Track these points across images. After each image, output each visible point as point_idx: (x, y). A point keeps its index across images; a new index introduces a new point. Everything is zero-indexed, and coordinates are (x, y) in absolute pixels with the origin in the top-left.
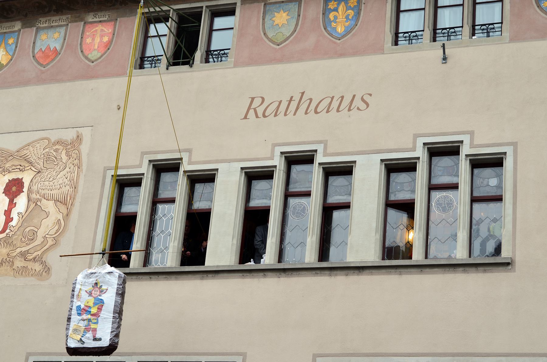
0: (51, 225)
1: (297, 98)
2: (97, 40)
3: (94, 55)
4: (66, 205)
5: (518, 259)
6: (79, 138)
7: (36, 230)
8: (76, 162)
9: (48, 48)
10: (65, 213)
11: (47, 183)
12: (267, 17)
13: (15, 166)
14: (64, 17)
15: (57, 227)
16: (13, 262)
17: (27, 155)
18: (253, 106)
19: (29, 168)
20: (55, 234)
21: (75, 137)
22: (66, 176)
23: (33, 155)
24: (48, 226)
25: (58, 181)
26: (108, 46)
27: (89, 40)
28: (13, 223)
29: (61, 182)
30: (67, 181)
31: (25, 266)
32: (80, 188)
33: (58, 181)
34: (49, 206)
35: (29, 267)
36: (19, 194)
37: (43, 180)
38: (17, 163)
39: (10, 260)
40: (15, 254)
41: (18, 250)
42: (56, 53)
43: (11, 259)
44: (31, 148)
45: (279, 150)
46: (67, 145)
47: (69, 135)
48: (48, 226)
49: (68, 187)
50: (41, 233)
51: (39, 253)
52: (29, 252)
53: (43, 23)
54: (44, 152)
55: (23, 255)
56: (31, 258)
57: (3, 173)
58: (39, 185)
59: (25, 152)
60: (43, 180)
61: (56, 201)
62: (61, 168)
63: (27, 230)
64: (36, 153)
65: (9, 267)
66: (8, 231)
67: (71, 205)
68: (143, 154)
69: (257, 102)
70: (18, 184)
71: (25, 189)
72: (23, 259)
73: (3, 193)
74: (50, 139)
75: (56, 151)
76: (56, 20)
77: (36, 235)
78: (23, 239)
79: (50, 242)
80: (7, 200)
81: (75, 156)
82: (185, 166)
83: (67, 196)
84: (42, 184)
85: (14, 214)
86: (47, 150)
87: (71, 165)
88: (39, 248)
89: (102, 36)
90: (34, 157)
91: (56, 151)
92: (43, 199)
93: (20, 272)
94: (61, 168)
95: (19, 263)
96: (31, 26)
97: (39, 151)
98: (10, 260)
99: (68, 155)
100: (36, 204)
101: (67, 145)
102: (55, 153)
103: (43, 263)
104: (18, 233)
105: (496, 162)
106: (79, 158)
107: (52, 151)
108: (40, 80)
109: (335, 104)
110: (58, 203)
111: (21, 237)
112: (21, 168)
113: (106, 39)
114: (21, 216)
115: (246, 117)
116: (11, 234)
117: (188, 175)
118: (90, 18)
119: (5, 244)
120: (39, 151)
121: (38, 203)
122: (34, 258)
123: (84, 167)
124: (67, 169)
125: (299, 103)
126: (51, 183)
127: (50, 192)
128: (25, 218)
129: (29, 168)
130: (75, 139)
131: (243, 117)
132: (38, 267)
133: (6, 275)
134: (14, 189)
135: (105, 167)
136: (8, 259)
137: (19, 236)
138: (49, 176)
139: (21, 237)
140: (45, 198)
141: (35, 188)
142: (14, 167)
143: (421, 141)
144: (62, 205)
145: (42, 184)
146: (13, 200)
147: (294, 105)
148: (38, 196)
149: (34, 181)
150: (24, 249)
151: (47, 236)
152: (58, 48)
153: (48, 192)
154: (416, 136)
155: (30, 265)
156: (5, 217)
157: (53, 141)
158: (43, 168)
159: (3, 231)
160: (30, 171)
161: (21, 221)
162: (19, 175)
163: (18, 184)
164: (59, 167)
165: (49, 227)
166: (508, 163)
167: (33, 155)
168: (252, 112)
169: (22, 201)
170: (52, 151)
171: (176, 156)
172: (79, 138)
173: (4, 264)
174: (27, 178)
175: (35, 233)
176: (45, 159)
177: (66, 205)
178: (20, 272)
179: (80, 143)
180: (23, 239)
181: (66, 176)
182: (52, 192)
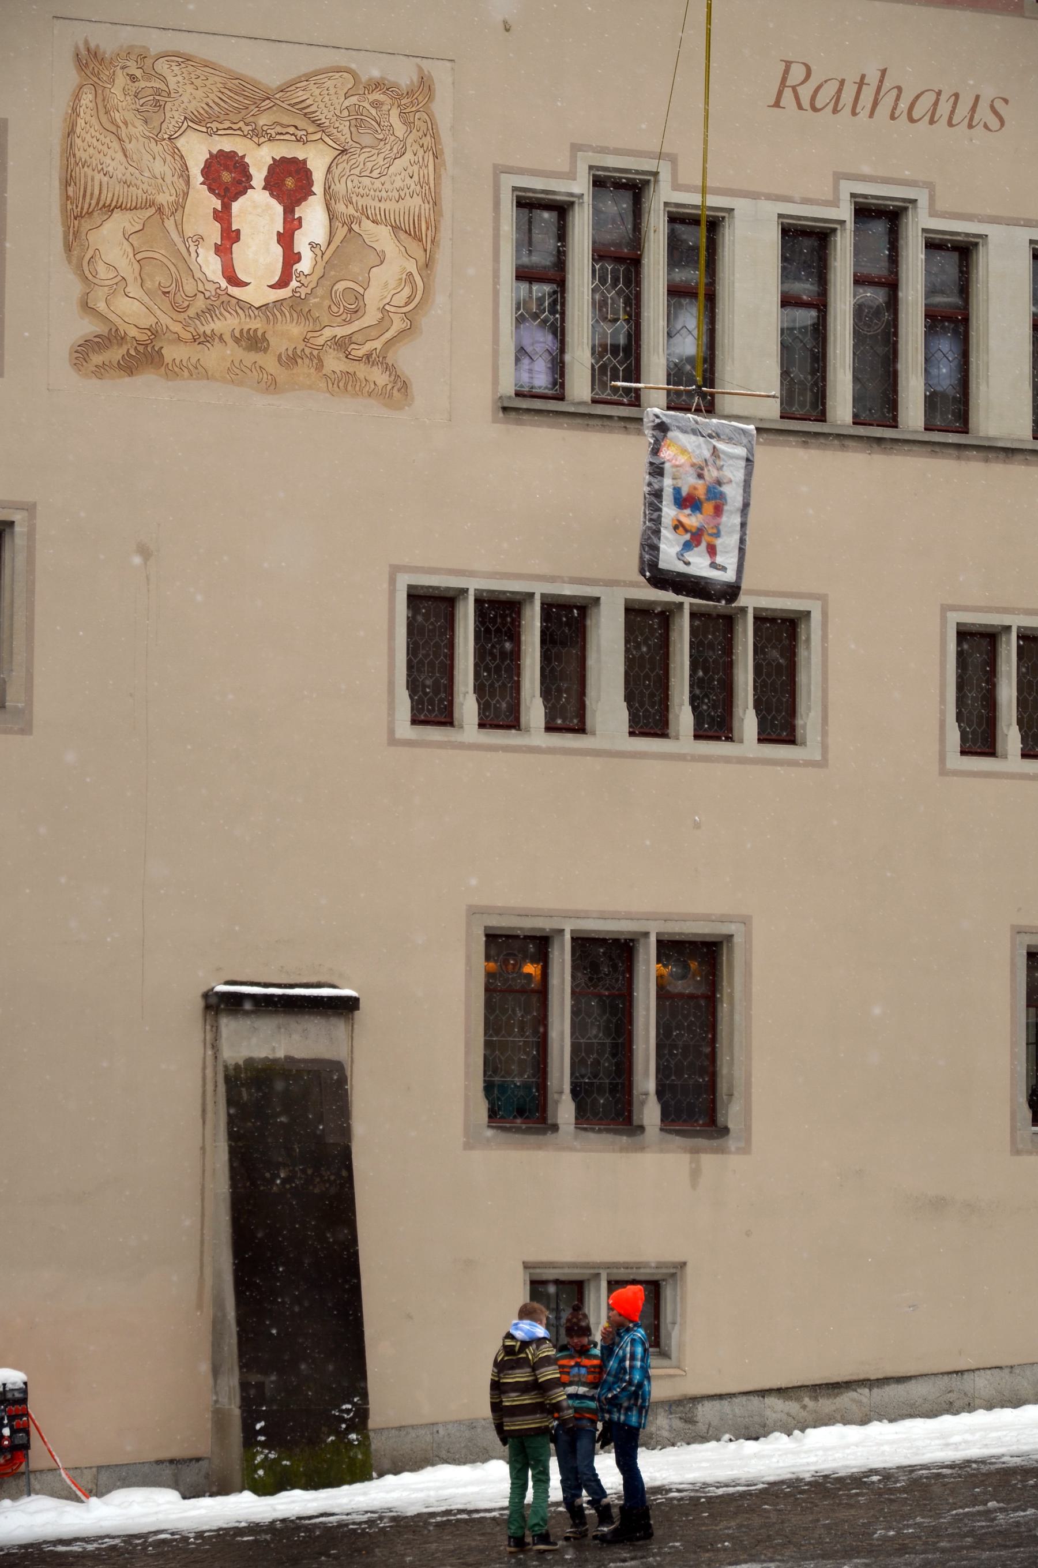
0: (392, 284)
4: (420, 240)
6: (427, 85)
7: (361, 291)
8: (427, 141)
10: (422, 262)
11: (366, 181)
13: (281, 125)
15: (407, 291)
16: (320, 360)
17: (308, 102)
18: (789, 82)
19: (318, 136)
20: (407, 304)
21: (415, 79)
22: (410, 171)
23: (322, 105)
24: (386, 284)
25: (393, 180)
28: (305, 266)
29: (398, 184)
30: (413, 186)
31: (351, 370)
32: (446, 206)
34: (381, 237)
35: (361, 375)
36: (305, 199)
37: (356, 171)
38: (286, 120)
39: (311, 353)
40: (321, 341)
41: (328, 333)
43: (315, 352)
44: (312, 86)
46: (400, 97)
48: (386, 284)
49: (417, 200)
50: (373, 297)
51: (378, 344)
52: (354, 339)
54: (347, 103)
55: (342, 344)
56: (360, 353)
57: (256, 139)
58: (349, 183)
59: (301, 95)
60: (356, 171)
61: (396, 228)
62: (395, 150)
63: (341, 286)
64: (329, 101)
65: (313, 370)
66: (294, 284)
67: (433, 242)
69: (797, 73)
70: (298, 172)
71: (318, 188)
72: (342, 355)
73: (264, 188)
74: (354, 71)
75: (376, 105)
77: (361, 303)
78: (335, 309)
80: (279, 209)
81: (424, 128)
83: (419, 220)
84: (356, 182)
85: (301, 244)
86: (353, 100)
87: (416, 147)
88: (374, 333)
90: (325, 111)
91: (376, 105)
92: (364, 218)
93: (341, 384)
94: (395, 150)
95: (334, 362)
97: (334, 97)
98: (311, 353)
100: (350, 230)
101: (400, 97)
102: (373, 111)
103: (389, 368)
104: (320, 291)
107: (366, 105)
110: (402, 236)
111: (327, 303)
112: (299, 133)
114: (319, 254)
115: (777, 104)
116: (303, 292)
117: (669, 212)
119: (295, 315)
120: (334, 97)
121: (355, 227)
122: (368, 356)
123: (448, 156)
124: (409, 155)
126: (378, 184)
127: (378, 205)
129: (318, 136)
130: (416, 83)
131: (772, 103)
132: (379, 377)
133: (310, 387)
134: (290, 182)
135: (495, 167)
136: (307, 351)
137: (322, 298)
138: (369, 165)
139: (327, 303)
140: (368, 218)
141: (339, 188)
142: (279, 129)
144: (410, 239)
145: (356, 182)
146: (293, 212)
148: (351, 211)
149: (336, 172)
150: (341, 332)
151: (387, 307)
153: (373, 203)
155: (362, 370)
156: (279, 250)
157: (364, 79)
158: (351, 142)
160: (321, 145)
161: (321, 264)
162: (298, 152)
163: (298, 172)
164: (388, 147)
165: (391, 287)
167: (322, 105)
169: (314, 217)
170: (366, 105)
171: (647, 165)
172: (425, 85)
173: (299, 361)
174: (318, 161)
175: (359, 297)
176: (353, 122)
177: (420, 240)
178: (341, 384)
179: (431, 98)
180: (335, 309)
181: (410, 171)
182: (383, 205)
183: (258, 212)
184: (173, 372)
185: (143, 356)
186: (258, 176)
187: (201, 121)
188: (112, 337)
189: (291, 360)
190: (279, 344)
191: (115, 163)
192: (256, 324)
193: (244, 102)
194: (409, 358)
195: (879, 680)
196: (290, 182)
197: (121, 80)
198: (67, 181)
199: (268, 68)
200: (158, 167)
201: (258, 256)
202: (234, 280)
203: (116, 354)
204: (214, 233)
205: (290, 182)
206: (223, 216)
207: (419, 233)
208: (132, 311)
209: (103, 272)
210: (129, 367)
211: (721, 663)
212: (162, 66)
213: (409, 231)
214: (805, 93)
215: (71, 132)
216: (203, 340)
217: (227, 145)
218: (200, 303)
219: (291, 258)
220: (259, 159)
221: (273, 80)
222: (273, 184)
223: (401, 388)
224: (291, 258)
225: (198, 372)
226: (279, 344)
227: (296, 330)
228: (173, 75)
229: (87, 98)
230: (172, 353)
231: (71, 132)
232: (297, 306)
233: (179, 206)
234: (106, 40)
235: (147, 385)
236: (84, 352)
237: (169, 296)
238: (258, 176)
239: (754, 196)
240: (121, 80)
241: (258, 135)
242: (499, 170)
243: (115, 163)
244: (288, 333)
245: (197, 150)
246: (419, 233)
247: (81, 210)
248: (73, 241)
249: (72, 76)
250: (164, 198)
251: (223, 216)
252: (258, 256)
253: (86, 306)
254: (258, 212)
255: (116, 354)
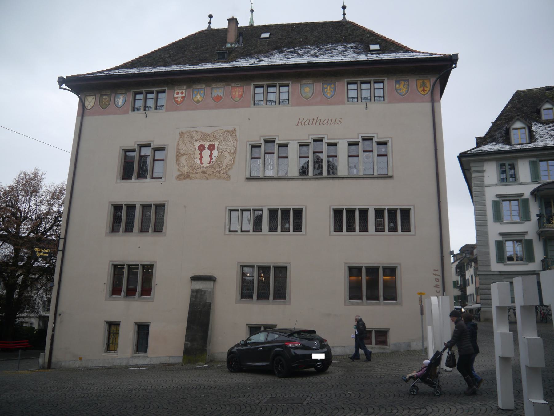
1: (316, 119)
2: (237, 94)
3: (237, 99)
5: (395, 175)
9: (218, 95)
12: (302, 89)
14: (223, 84)
25: (229, 145)
26: (241, 96)
27: (234, 93)
28: (213, 160)
33: (229, 145)
34: (227, 154)
42: (221, 98)
45: (311, 137)
47: (231, 129)
50: (225, 164)
53: (214, 85)
55: (219, 172)
68: (261, 136)
69: (301, 120)
71: (216, 148)
76: (219, 85)
79: (229, 167)
82: (277, 141)
85: (213, 157)
89: (239, 92)
95: (218, 175)
96: (210, 87)
99: (231, 135)
105: (385, 143)
106: (236, 137)
108: (216, 107)
109: (329, 122)
113: (240, 93)
118: (233, 85)
125: (316, 121)
128: (218, 159)
132: (225, 176)
141: (220, 147)
143: (360, 136)
147: (315, 122)
152: (222, 96)
154: (359, 134)
155: (222, 175)
159: (210, 163)
162: (213, 143)
166: (389, 144)
168: (300, 123)
169: (215, 152)
172: (235, 130)
175: (222, 164)
183: (206, 153)
184: (191, 179)
185: (187, 176)
186: (207, 147)
187: (198, 140)
188: (183, 174)
189: (211, 175)
190: (208, 173)
191: (185, 148)
192: (205, 170)
193: (205, 136)
194: (230, 173)
195: (318, 219)
196: (212, 148)
197: (186, 136)
198: (177, 152)
199: (208, 131)
200: (191, 148)
201: (206, 159)
202: (202, 163)
203: (183, 177)
204: (199, 157)
205: (212, 148)
206: (201, 154)
207: (233, 153)
208: (185, 170)
209: (182, 165)
210: (184, 179)
211: (289, 219)
212: (192, 133)
213: (231, 153)
214: (303, 123)
215: (178, 144)
216: (196, 173)
217: (202, 143)
218: (196, 168)
219: (211, 159)
220: (207, 145)
221: (209, 133)
222: (209, 148)
223: (229, 177)
224: (211, 159)
225: (195, 178)
226: (208, 173)
227: (211, 170)
228: (194, 134)
229: (181, 139)
230: (191, 176)
231: (178, 144)
232: (212, 166)
233: (194, 153)
234: (184, 130)
235: (188, 181)
236: (178, 177)
237: (192, 167)
238: (207, 147)
239: (293, 140)
240: (186, 136)
241: (207, 141)
242: (247, 141)
243: (185, 148)
244: (211, 170)
245: (197, 145)
246: (233, 153)
247: (179, 156)
248: (177, 160)
249: (178, 136)
250: (191, 153)
251: (201, 154)
252: (206, 159)
253: (179, 170)
254: (206, 153)
255: (183, 177)
